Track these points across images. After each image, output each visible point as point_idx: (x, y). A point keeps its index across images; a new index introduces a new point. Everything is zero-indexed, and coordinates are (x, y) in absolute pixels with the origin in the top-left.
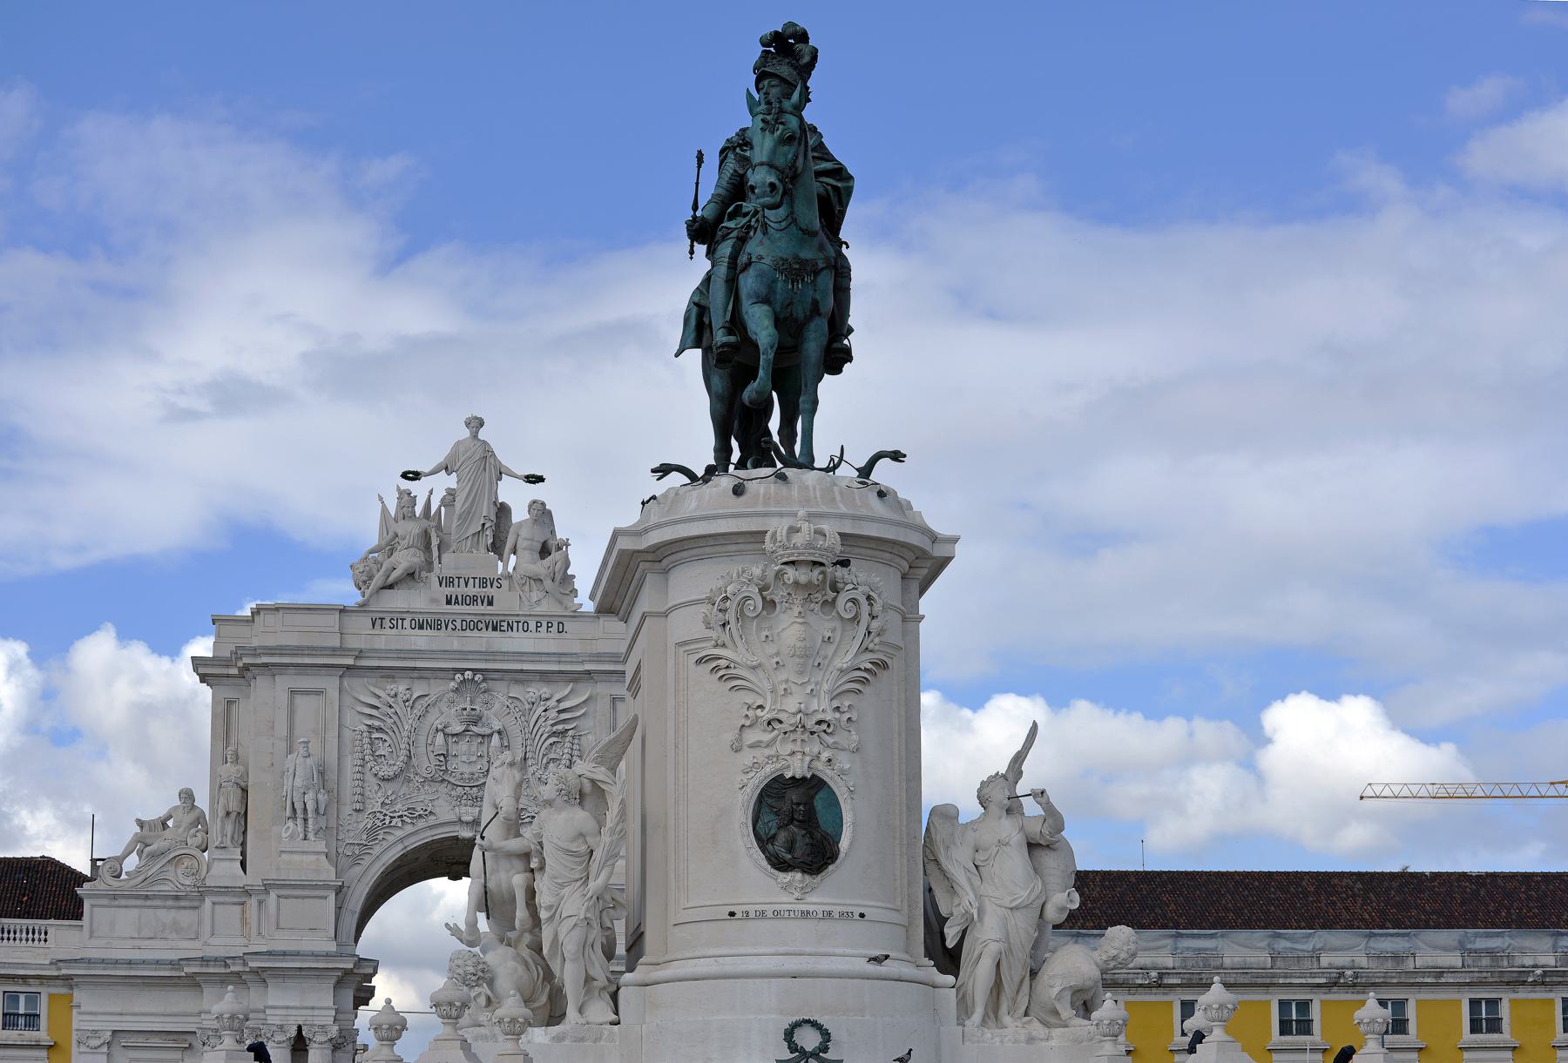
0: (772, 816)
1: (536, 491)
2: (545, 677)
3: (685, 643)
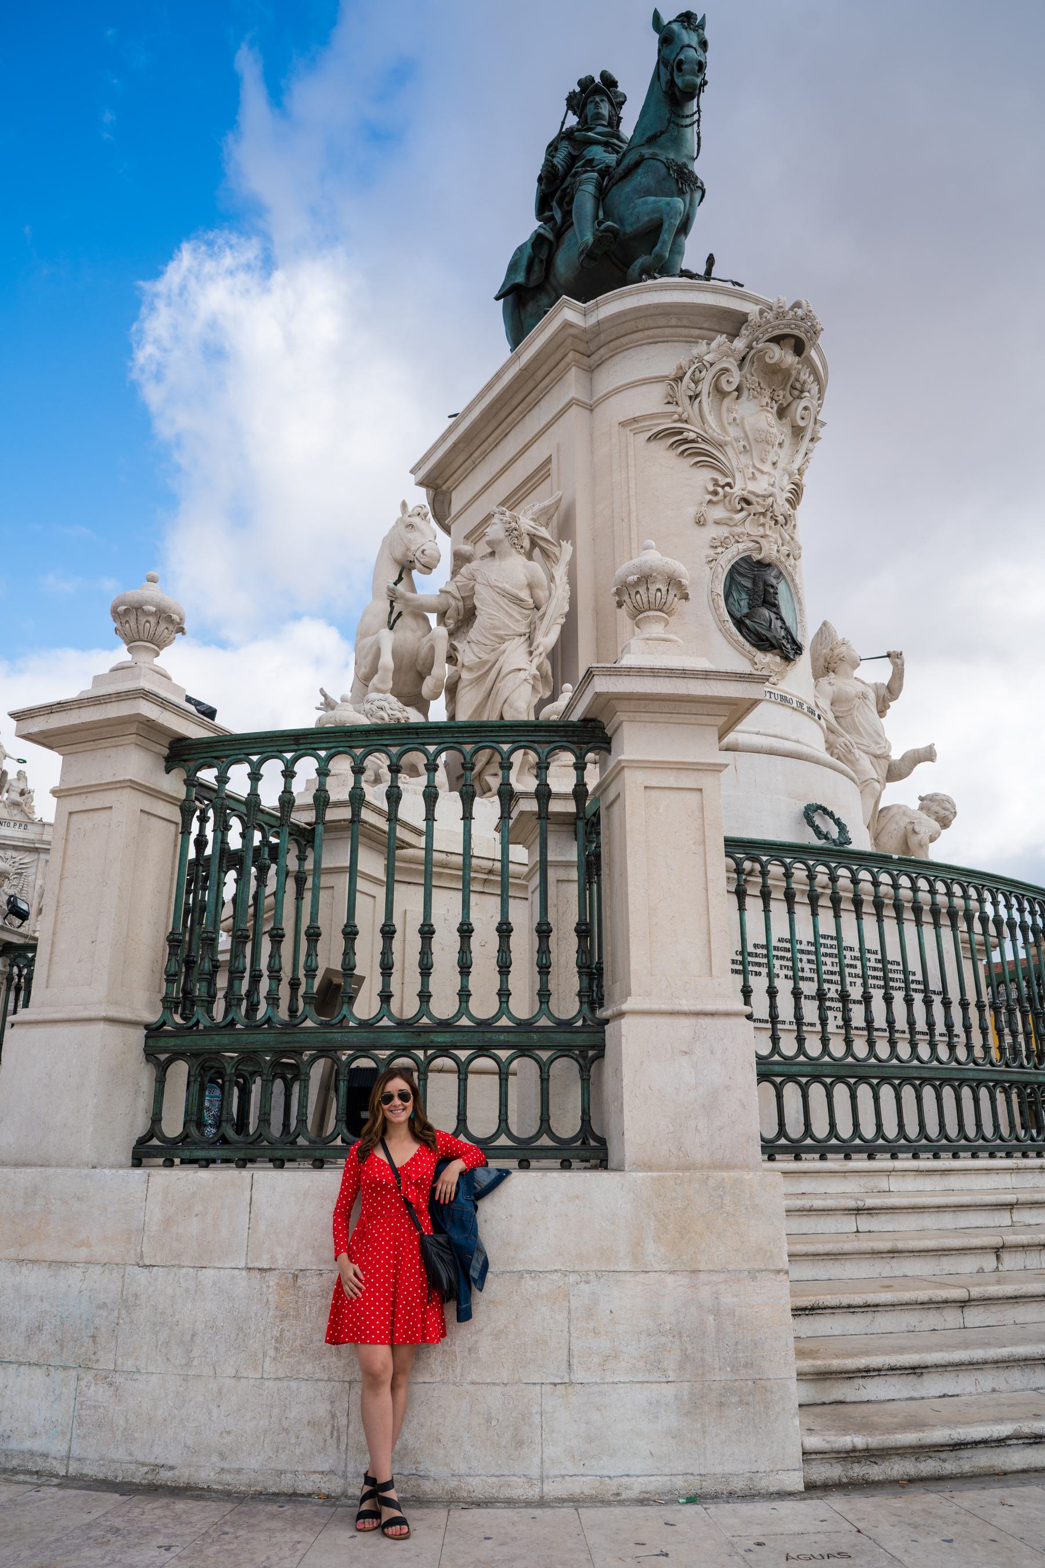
0: (744, 596)
1: (21, 767)
2: (15, 848)
3: (635, 420)
